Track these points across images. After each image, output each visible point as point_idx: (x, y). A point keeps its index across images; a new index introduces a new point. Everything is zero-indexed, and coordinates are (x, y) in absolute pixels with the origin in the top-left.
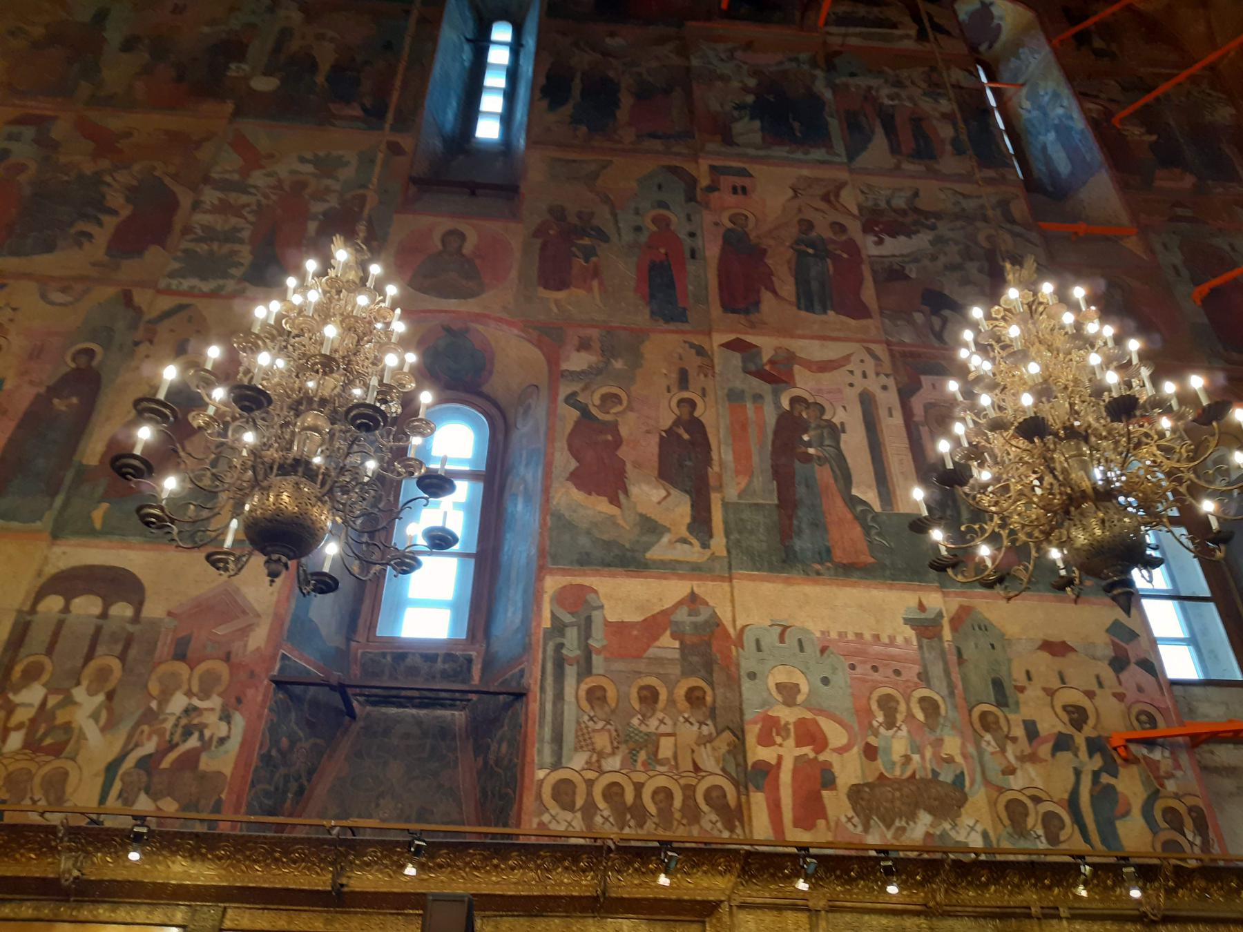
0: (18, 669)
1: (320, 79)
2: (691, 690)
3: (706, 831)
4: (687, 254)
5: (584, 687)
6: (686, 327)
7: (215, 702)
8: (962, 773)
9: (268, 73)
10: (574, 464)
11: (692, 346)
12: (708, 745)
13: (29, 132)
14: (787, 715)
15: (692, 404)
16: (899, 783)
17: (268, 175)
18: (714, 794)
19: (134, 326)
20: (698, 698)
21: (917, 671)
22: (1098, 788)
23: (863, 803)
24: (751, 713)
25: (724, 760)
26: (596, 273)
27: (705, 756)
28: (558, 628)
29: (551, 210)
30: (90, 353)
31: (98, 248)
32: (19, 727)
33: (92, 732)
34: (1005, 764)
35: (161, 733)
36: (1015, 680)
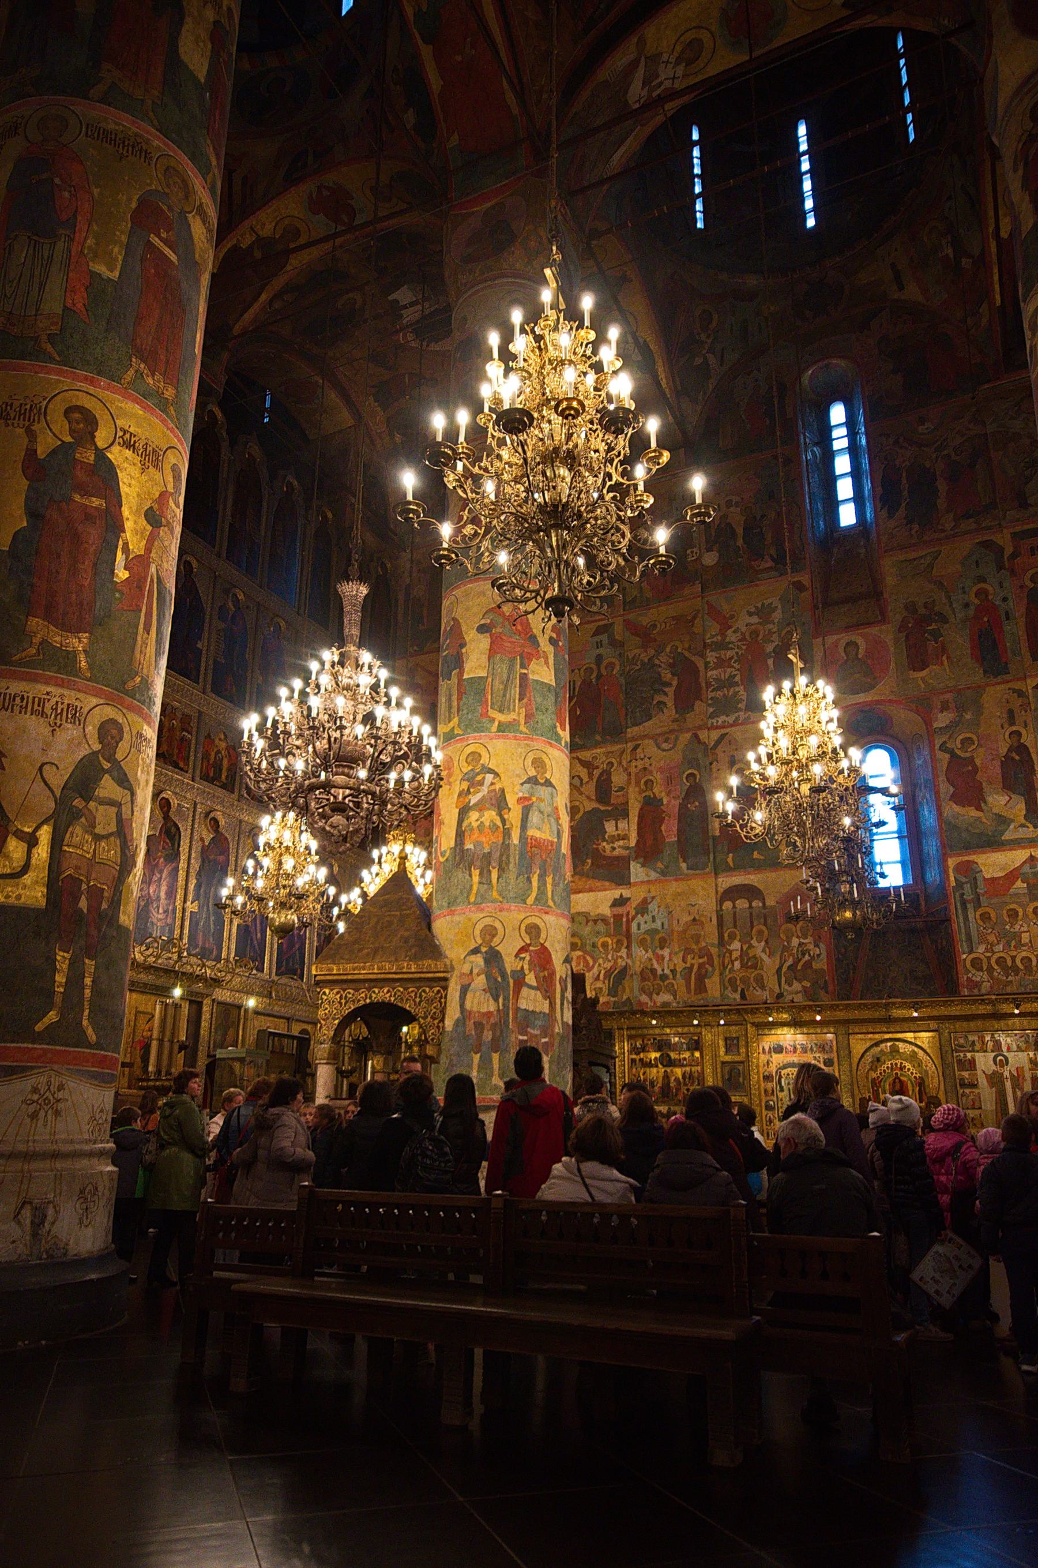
0: (726, 935)
1: (740, 542)
4: (1003, 617)
5: (978, 913)
6: (1007, 677)
7: (809, 940)
9: (709, 550)
10: (952, 789)
11: (1014, 691)
13: (604, 638)
15: (1020, 734)
17: (735, 632)
19: (706, 755)
26: (944, 650)
28: (960, 885)
29: (906, 608)
30: (691, 774)
31: (670, 711)
32: (736, 959)
33: (765, 957)
35: (792, 955)
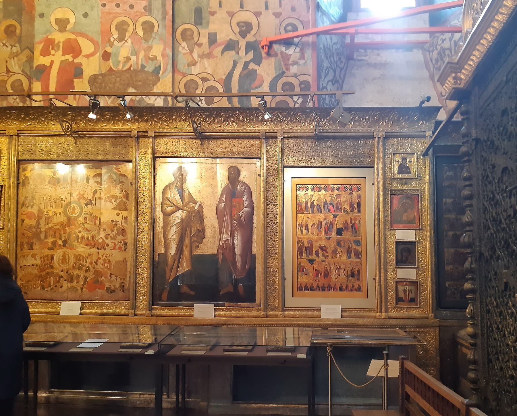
2: (8, 27)
3: (11, 103)
8: (160, 66)
12: (16, 58)
14: (60, 37)
16: (120, 73)
18: (16, 84)
20: (12, 31)
21: (144, 5)
22: (245, 72)
23: (97, 85)
24: (39, 37)
25: (23, 65)
27: (13, 63)
34: (190, 59)
36: (210, 8)
